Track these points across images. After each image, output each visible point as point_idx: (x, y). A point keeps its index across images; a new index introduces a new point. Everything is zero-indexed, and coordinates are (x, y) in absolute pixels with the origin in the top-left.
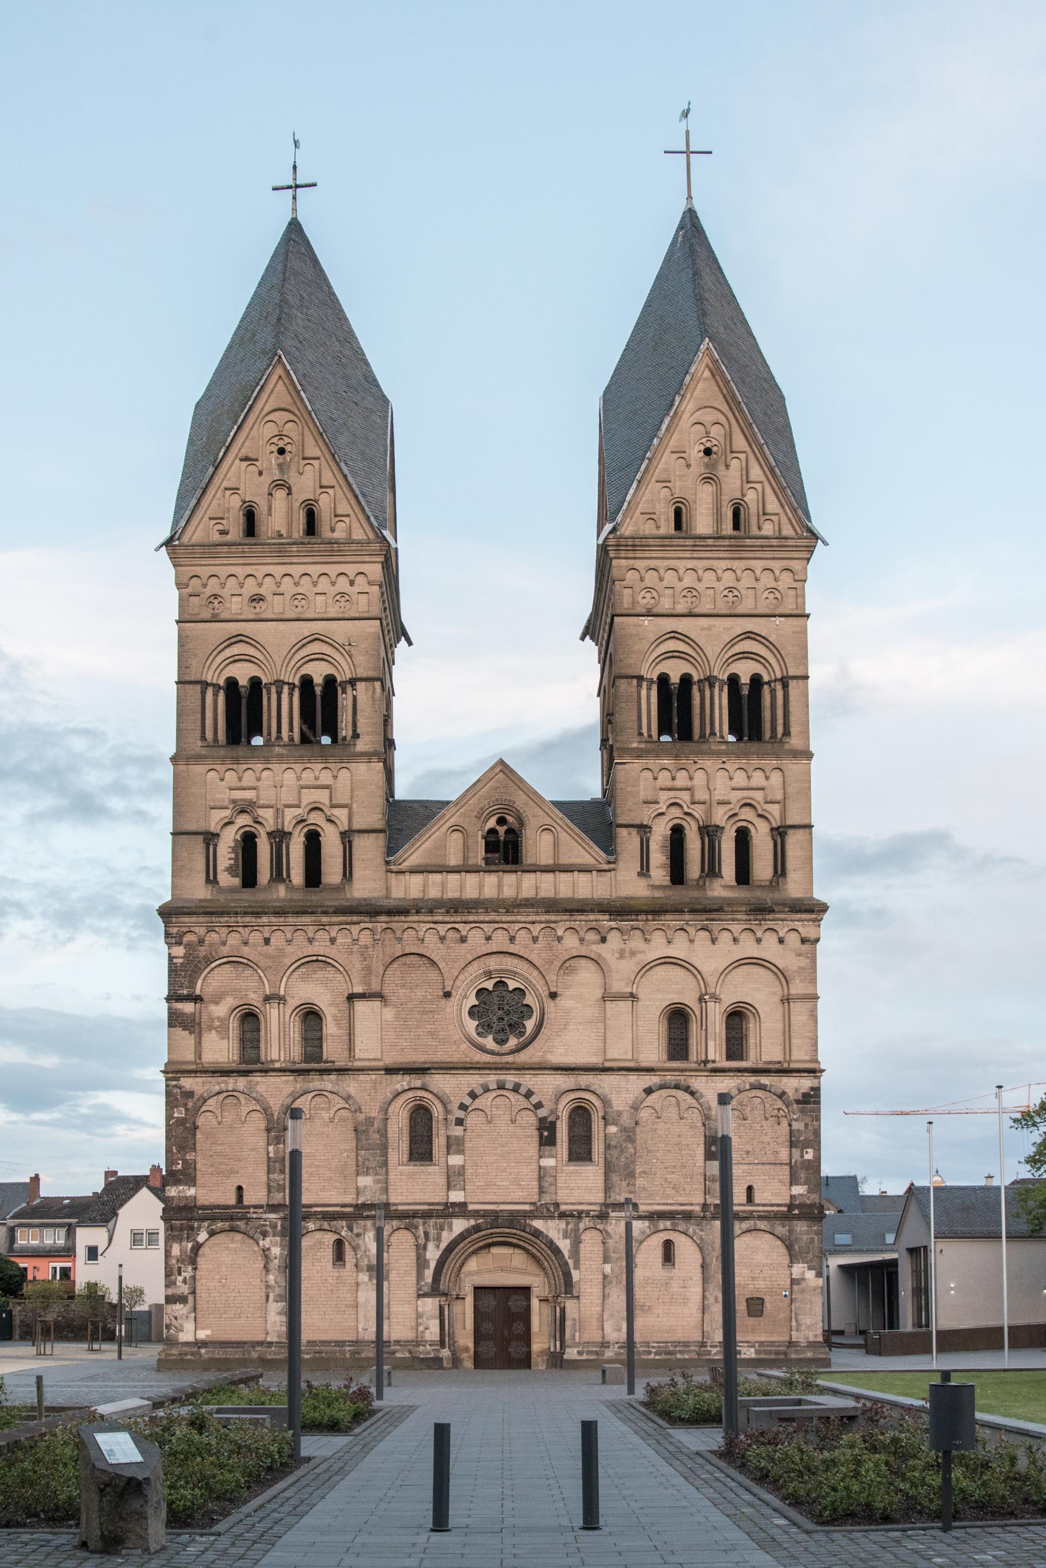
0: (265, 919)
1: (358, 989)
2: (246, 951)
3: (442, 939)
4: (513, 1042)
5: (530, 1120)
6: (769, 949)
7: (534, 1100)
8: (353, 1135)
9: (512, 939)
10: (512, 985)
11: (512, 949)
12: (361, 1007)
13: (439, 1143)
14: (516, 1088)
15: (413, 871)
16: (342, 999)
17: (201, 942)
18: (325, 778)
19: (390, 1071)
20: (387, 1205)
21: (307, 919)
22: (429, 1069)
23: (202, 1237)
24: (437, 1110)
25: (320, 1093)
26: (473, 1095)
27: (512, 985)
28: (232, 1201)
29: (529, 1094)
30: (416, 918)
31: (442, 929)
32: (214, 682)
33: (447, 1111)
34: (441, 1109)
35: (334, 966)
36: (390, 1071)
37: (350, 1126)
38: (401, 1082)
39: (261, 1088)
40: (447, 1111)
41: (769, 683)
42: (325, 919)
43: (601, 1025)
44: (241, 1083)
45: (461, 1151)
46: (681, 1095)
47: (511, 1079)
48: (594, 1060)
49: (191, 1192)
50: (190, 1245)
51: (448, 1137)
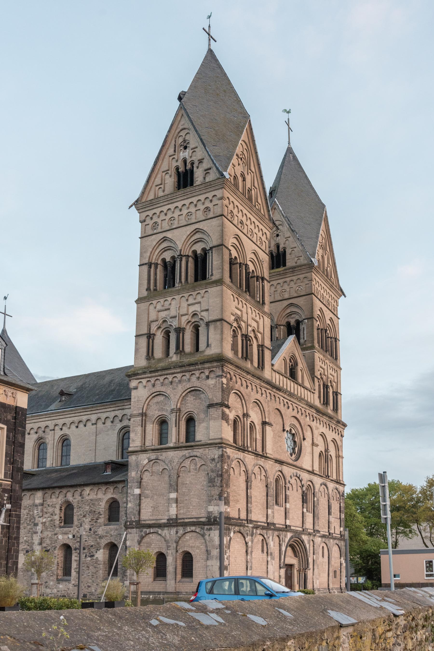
0: (249, 377)
1: (267, 420)
2: (242, 389)
3: (284, 405)
4: (294, 456)
5: (300, 491)
6: (337, 438)
7: (303, 483)
8: (265, 489)
9: (298, 412)
10: (293, 432)
11: (298, 416)
12: (268, 428)
13: (282, 498)
14: (299, 478)
15: (277, 372)
16: (260, 422)
17: (231, 379)
18: (257, 318)
19: (277, 461)
20: (274, 524)
21: (258, 381)
22: (283, 463)
23: (232, 534)
24: (282, 482)
25: (261, 467)
26: (291, 477)
27: (293, 432)
28: (237, 517)
29: (301, 481)
30: (281, 393)
31: (286, 401)
32: (184, 254)
33: (285, 483)
34: (283, 482)
35: (259, 406)
36: (277, 461)
37: (265, 485)
38: (278, 467)
39: (247, 460)
40: (285, 483)
41: (331, 338)
42: (262, 384)
43: (312, 455)
44: (241, 455)
45: (289, 502)
46: (326, 489)
47: (299, 472)
48: (310, 469)
49: (228, 510)
50: (229, 538)
51: (286, 495)
